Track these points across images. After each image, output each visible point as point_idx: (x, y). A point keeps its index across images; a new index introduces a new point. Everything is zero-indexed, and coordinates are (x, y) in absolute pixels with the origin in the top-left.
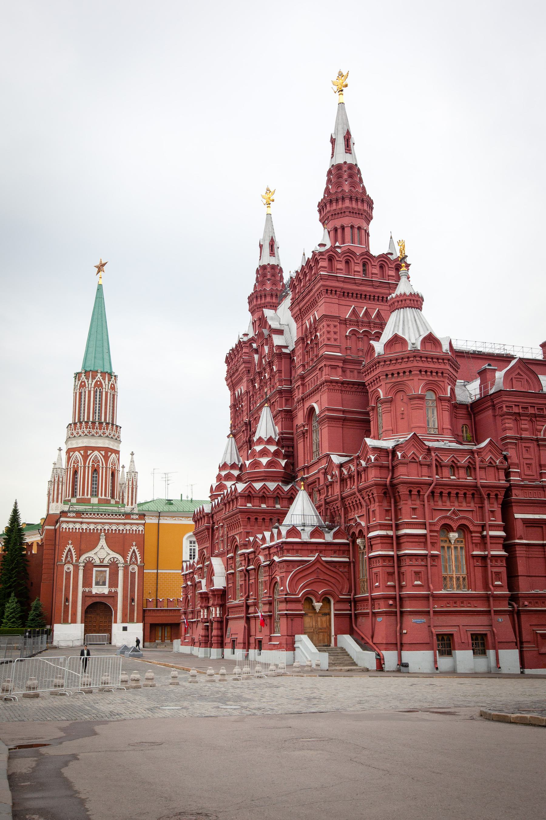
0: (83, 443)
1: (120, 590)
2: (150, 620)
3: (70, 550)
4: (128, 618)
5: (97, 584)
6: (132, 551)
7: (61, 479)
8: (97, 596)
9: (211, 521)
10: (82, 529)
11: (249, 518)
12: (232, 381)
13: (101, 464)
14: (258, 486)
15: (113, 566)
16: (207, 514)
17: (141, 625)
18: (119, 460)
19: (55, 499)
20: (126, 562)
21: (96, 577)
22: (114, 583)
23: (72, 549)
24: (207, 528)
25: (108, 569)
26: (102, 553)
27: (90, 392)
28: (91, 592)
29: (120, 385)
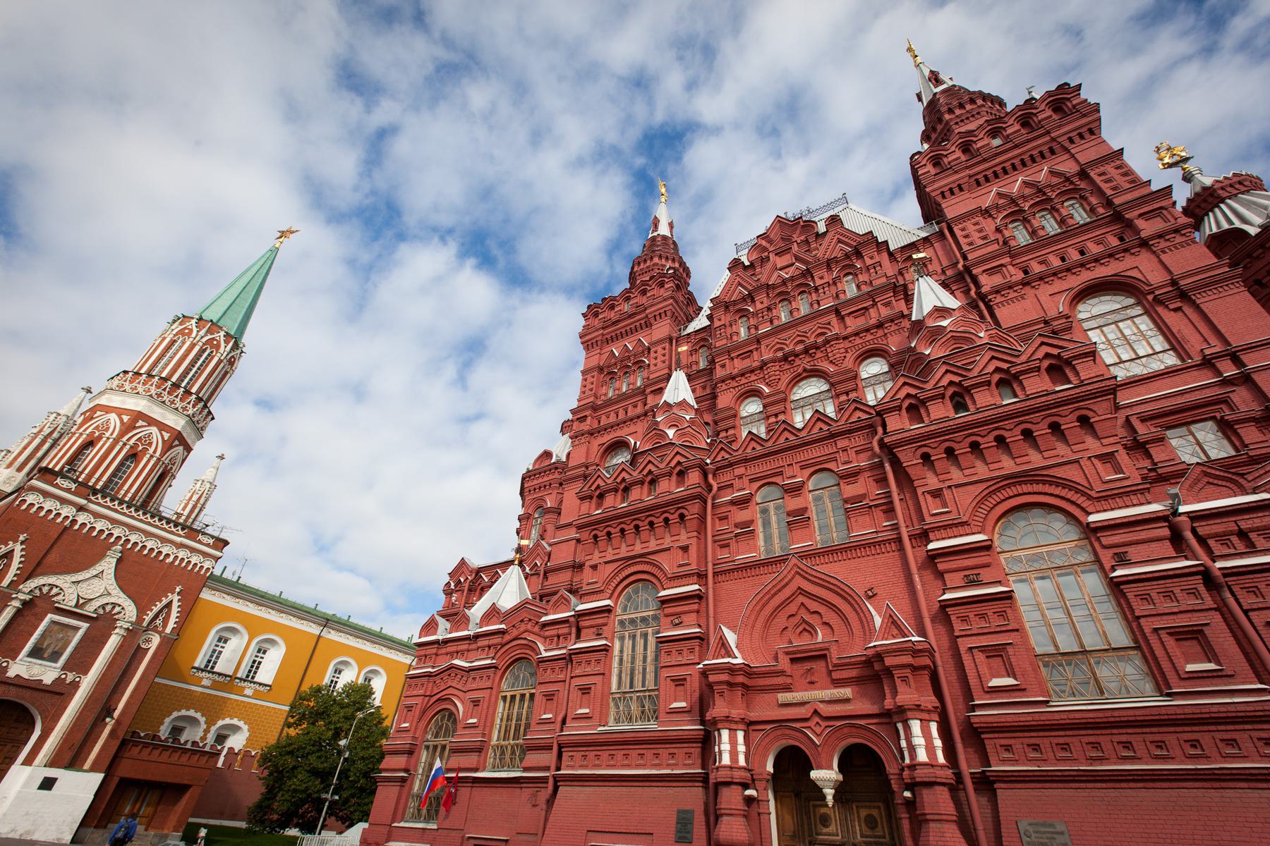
1: (88, 682)
2: (126, 769)
5: (36, 653)
6: (165, 601)
7: (55, 435)
8: (19, 683)
10: (74, 522)
13: (151, 451)
15: (102, 623)
18: (184, 461)
19: (17, 464)
20: (140, 619)
21: (43, 636)
22: (80, 662)
27: (193, 346)
29: (241, 365)
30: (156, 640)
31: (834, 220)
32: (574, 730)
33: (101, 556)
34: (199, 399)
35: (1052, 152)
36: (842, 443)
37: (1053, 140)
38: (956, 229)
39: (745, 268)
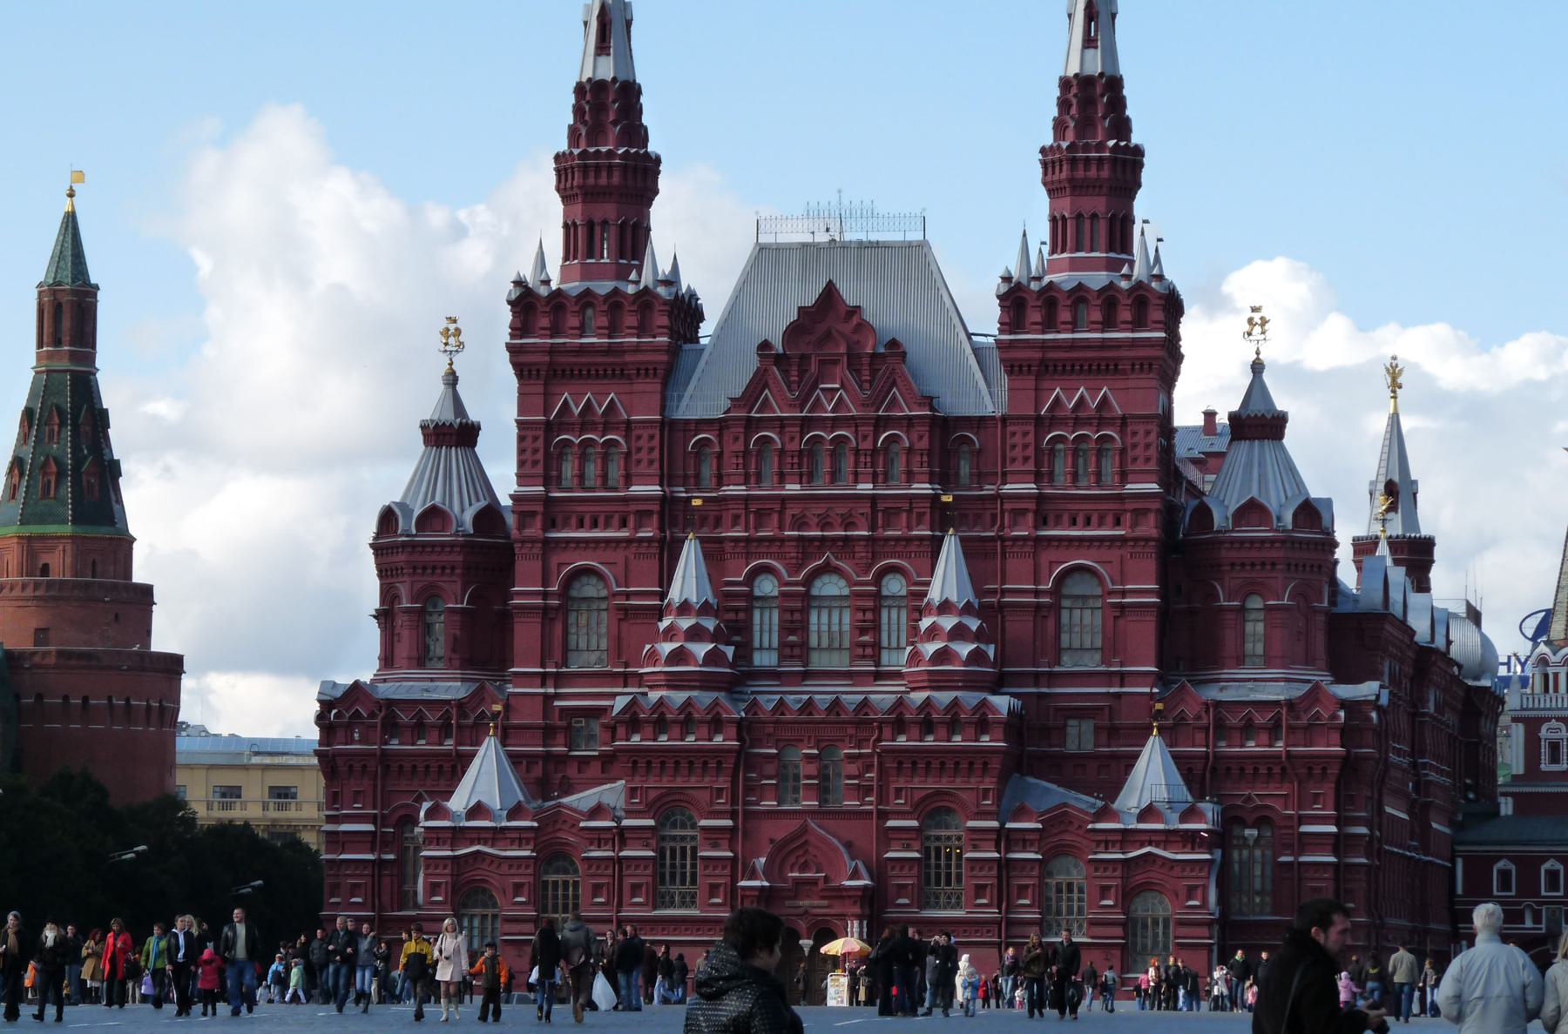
12: (551, 363)
31: (894, 344)
32: (626, 913)
35: (1116, 370)
36: (851, 731)
37: (1122, 359)
38: (1010, 429)
39: (779, 360)
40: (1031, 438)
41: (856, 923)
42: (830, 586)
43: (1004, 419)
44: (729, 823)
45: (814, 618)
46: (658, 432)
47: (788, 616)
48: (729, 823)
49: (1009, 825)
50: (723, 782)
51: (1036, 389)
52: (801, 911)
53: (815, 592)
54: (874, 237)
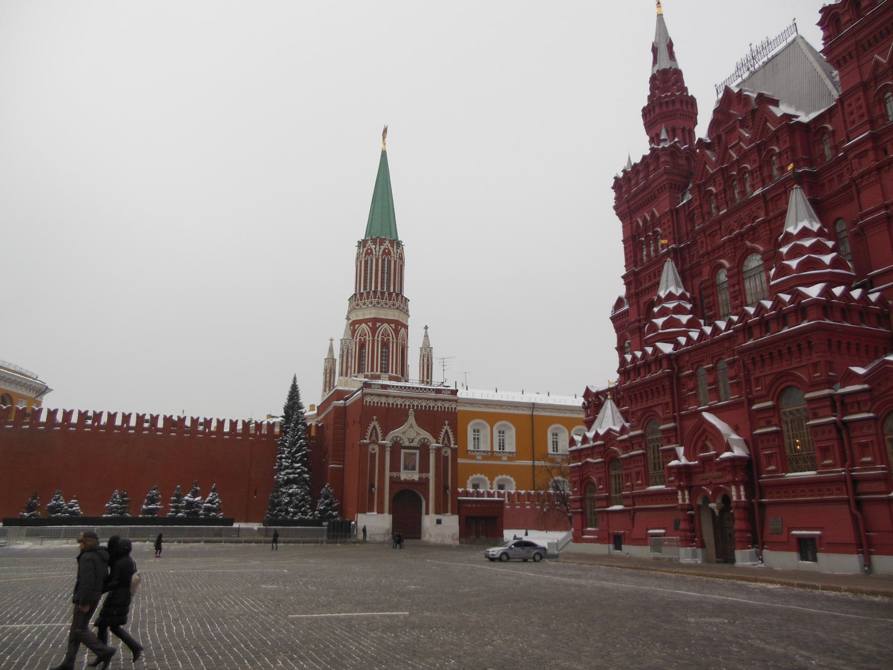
0: (371, 314)
3: (374, 428)
4: (441, 509)
5: (406, 468)
6: (444, 430)
8: (406, 482)
9: (676, 367)
10: (389, 404)
11: (829, 340)
12: (629, 207)
14: (838, 291)
15: (424, 448)
16: (668, 356)
17: (456, 518)
21: (405, 460)
22: (424, 468)
23: (377, 426)
24: (669, 376)
25: (417, 452)
26: (410, 432)
28: (399, 478)
30: (449, 452)
33: (407, 416)
34: (397, 295)
40: (862, 101)
41: (733, 489)
42: (754, 262)
43: (841, 101)
44: (672, 425)
45: (747, 285)
46: (669, 217)
47: (732, 290)
48: (672, 425)
49: (841, 391)
50: (668, 399)
51: (860, 67)
52: (707, 482)
53: (745, 269)
54: (770, 56)
